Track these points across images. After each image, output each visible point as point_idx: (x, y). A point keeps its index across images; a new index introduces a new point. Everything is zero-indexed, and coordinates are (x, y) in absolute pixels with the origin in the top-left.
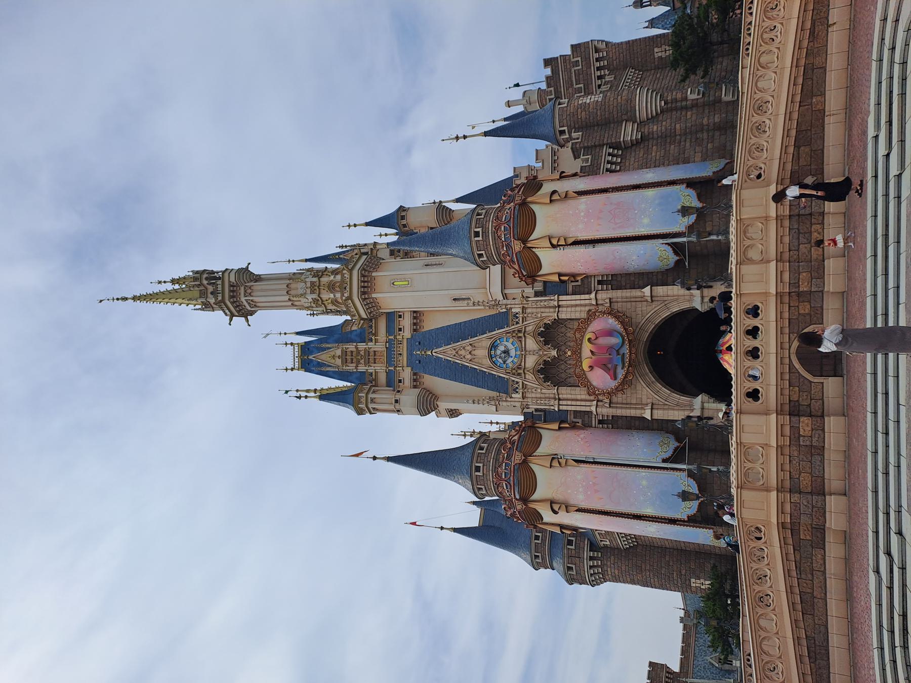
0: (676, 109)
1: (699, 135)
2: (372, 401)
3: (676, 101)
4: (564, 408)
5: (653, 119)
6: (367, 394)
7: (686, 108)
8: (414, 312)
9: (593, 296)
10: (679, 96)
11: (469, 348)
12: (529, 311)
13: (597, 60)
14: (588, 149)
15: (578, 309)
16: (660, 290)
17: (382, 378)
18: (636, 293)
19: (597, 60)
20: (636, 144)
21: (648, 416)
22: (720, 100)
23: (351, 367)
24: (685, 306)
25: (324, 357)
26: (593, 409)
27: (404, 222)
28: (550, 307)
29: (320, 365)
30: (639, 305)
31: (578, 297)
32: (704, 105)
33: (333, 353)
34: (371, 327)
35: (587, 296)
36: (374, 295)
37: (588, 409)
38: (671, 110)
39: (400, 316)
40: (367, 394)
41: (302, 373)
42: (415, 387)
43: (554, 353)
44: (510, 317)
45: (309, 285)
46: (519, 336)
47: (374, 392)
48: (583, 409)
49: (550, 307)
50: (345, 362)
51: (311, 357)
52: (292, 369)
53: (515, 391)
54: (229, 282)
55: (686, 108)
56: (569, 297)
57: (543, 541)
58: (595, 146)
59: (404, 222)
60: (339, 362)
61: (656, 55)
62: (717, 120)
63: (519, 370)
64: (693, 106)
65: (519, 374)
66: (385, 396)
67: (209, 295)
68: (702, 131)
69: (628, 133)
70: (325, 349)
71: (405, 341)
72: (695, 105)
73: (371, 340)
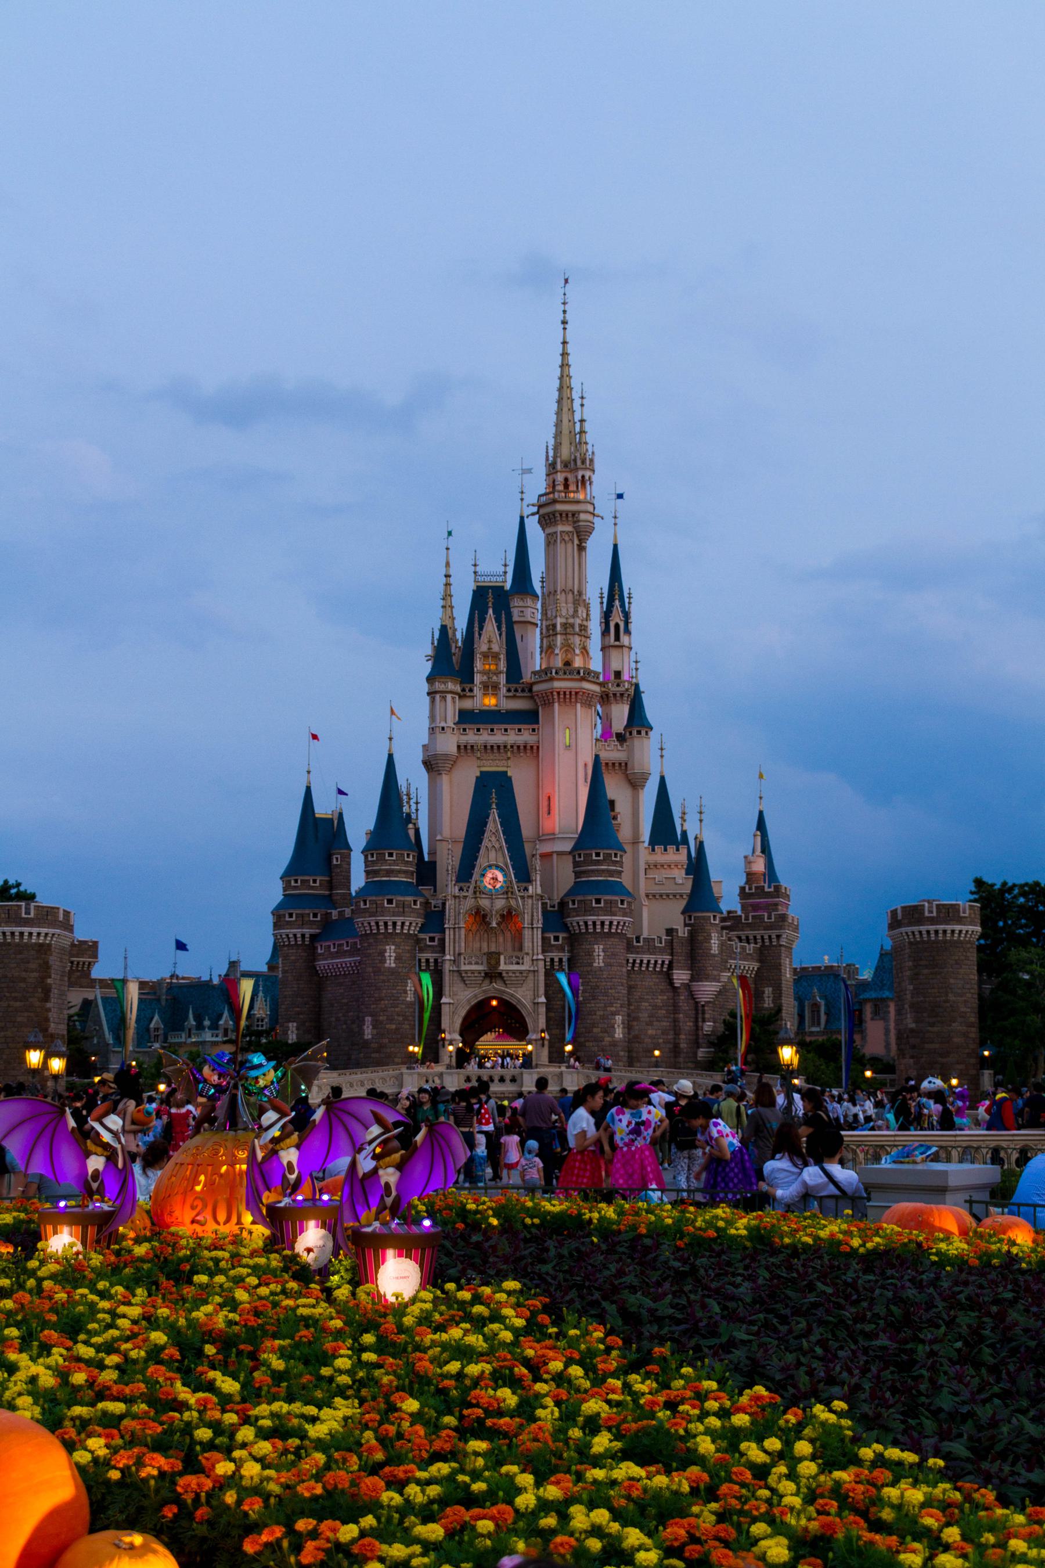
0: (697, 1014)
1: (672, 1032)
2: (444, 698)
3: (703, 1013)
4: (447, 932)
5: (692, 995)
6: (451, 692)
7: (696, 1021)
8: (538, 747)
9: (541, 957)
10: (707, 1016)
11: (497, 846)
12: (530, 901)
13: (770, 937)
14: (670, 944)
15: (530, 945)
16: (543, 1010)
17: (467, 704)
18: (542, 990)
19: (770, 937)
20: (671, 983)
21: (444, 1000)
22: (698, 1047)
23: (478, 665)
24: (530, 1026)
25: (490, 626)
26: (448, 957)
27: (635, 732)
28: (532, 920)
29: (482, 621)
30: (531, 993)
31: (540, 944)
32: (697, 1035)
33: (494, 640)
34: (523, 691)
35: (540, 951)
36: (556, 705)
37: (447, 952)
38: (696, 1010)
39: (534, 730)
40: (451, 692)
41: (472, 586)
42: (459, 747)
43: (494, 925)
44: (524, 885)
45: (571, 621)
46: (507, 892)
47: (453, 698)
48: (447, 949)
49: (532, 920)
50: (485, 656)
51: (491, 611)
52: (475, 573)
53: (461, 889)
54: (579, 512)
55: (696, 1021)
56: (540, 936)
57: (312, 888)
58: (672, 949)
59: (635, 732)
60: (484, 648)
61: (766, 989)
62: (682, 1046)
63: (478, 891)
64: (697, 1026)
65: (475, 893)
66: (451, 709)
67: (564, 475)
68: (675, 1034)
69: (681, 976)
70: (499, 628)
71: (504, 769)
72: (697, 1028)
73: (509, 690)
